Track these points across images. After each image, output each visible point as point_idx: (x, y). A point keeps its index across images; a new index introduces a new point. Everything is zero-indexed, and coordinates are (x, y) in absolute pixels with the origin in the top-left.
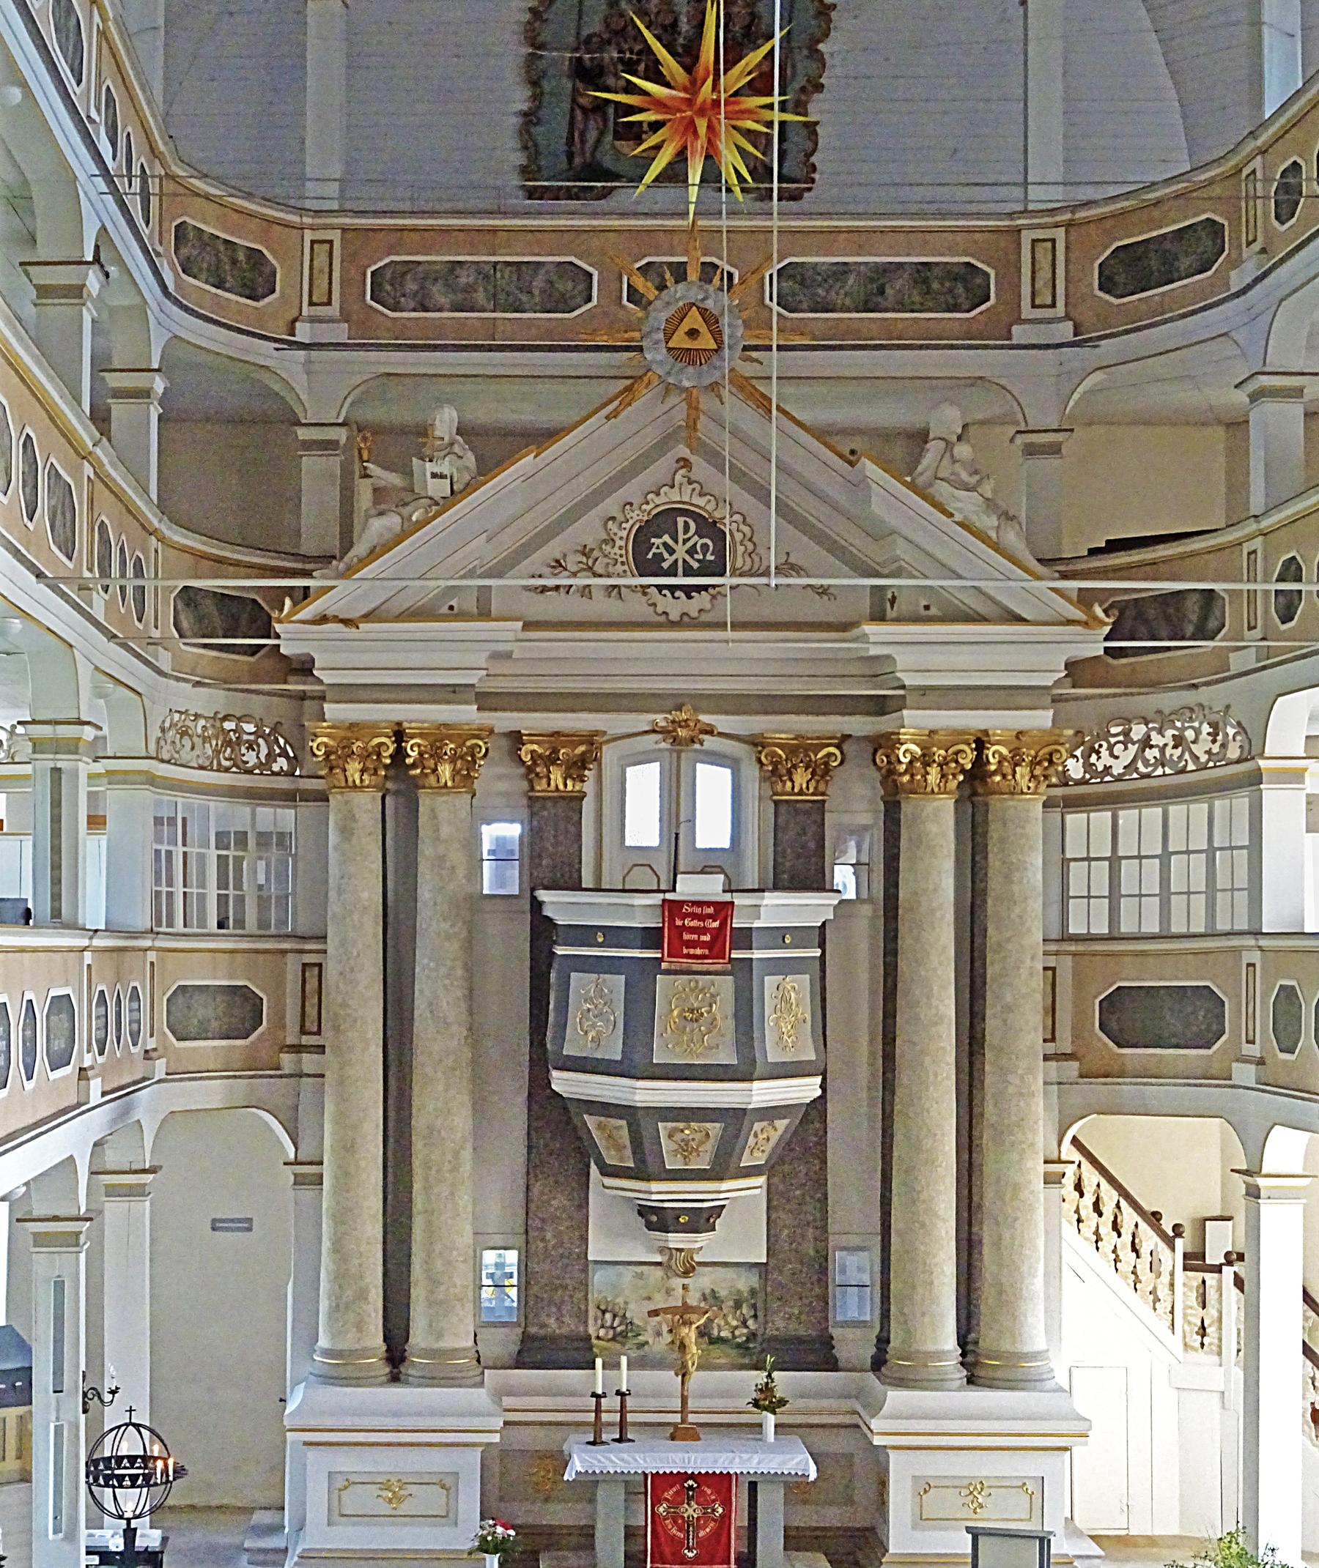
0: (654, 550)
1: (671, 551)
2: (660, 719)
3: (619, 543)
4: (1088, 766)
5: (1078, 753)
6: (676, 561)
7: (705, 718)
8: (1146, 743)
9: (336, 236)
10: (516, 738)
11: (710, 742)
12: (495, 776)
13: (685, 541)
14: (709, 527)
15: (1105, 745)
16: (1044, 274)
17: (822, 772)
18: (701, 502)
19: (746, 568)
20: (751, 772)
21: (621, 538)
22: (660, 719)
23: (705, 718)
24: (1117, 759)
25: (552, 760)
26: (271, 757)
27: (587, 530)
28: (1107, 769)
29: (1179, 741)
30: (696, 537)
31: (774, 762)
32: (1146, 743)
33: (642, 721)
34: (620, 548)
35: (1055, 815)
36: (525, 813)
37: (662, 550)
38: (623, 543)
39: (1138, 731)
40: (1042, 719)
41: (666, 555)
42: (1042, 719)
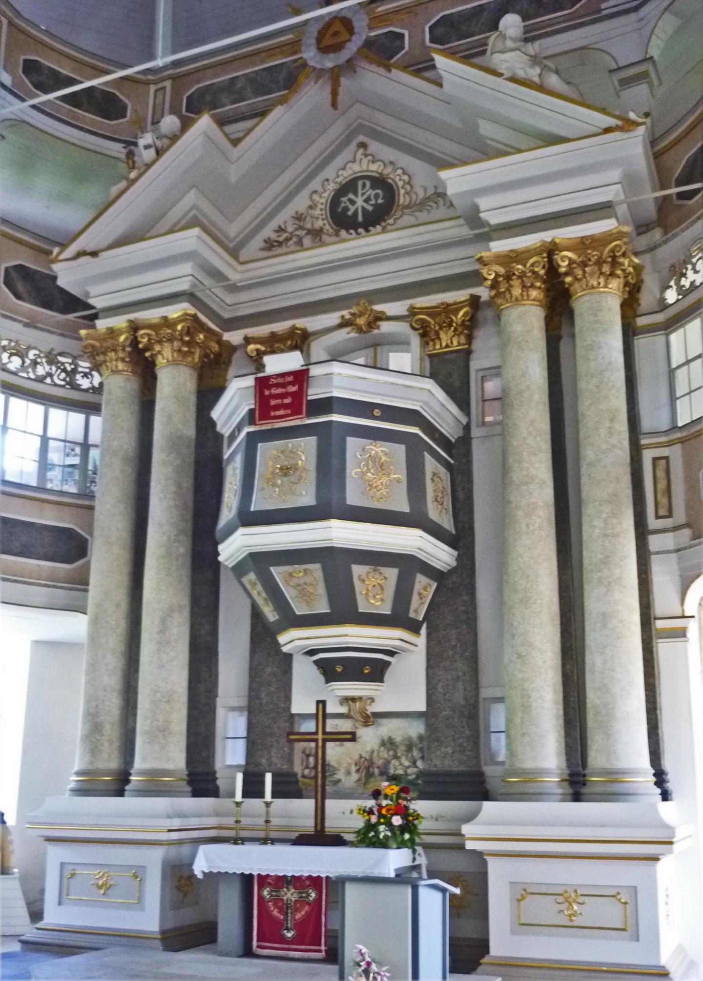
0: (343, 205)
1: (353, 202)
2: (346, 313)
3: (320, 206)
4: (680, 289)
5: (672, 283)
6: (357, 209)
7: (378, 308)
11: (386, 327)
13: (363, 194)
14: (379, 182)
15: (690, 267)
18: (374, 167)
19: (407, 203)
21: (322, 204)
23: (378, 308)
27: (300, 203)
28: (692, 283)
30: (370, 191)
33: (332, 318)
34: (321, 210)
37: (348, 204)
38: (323, 207)
41: (350, 206)
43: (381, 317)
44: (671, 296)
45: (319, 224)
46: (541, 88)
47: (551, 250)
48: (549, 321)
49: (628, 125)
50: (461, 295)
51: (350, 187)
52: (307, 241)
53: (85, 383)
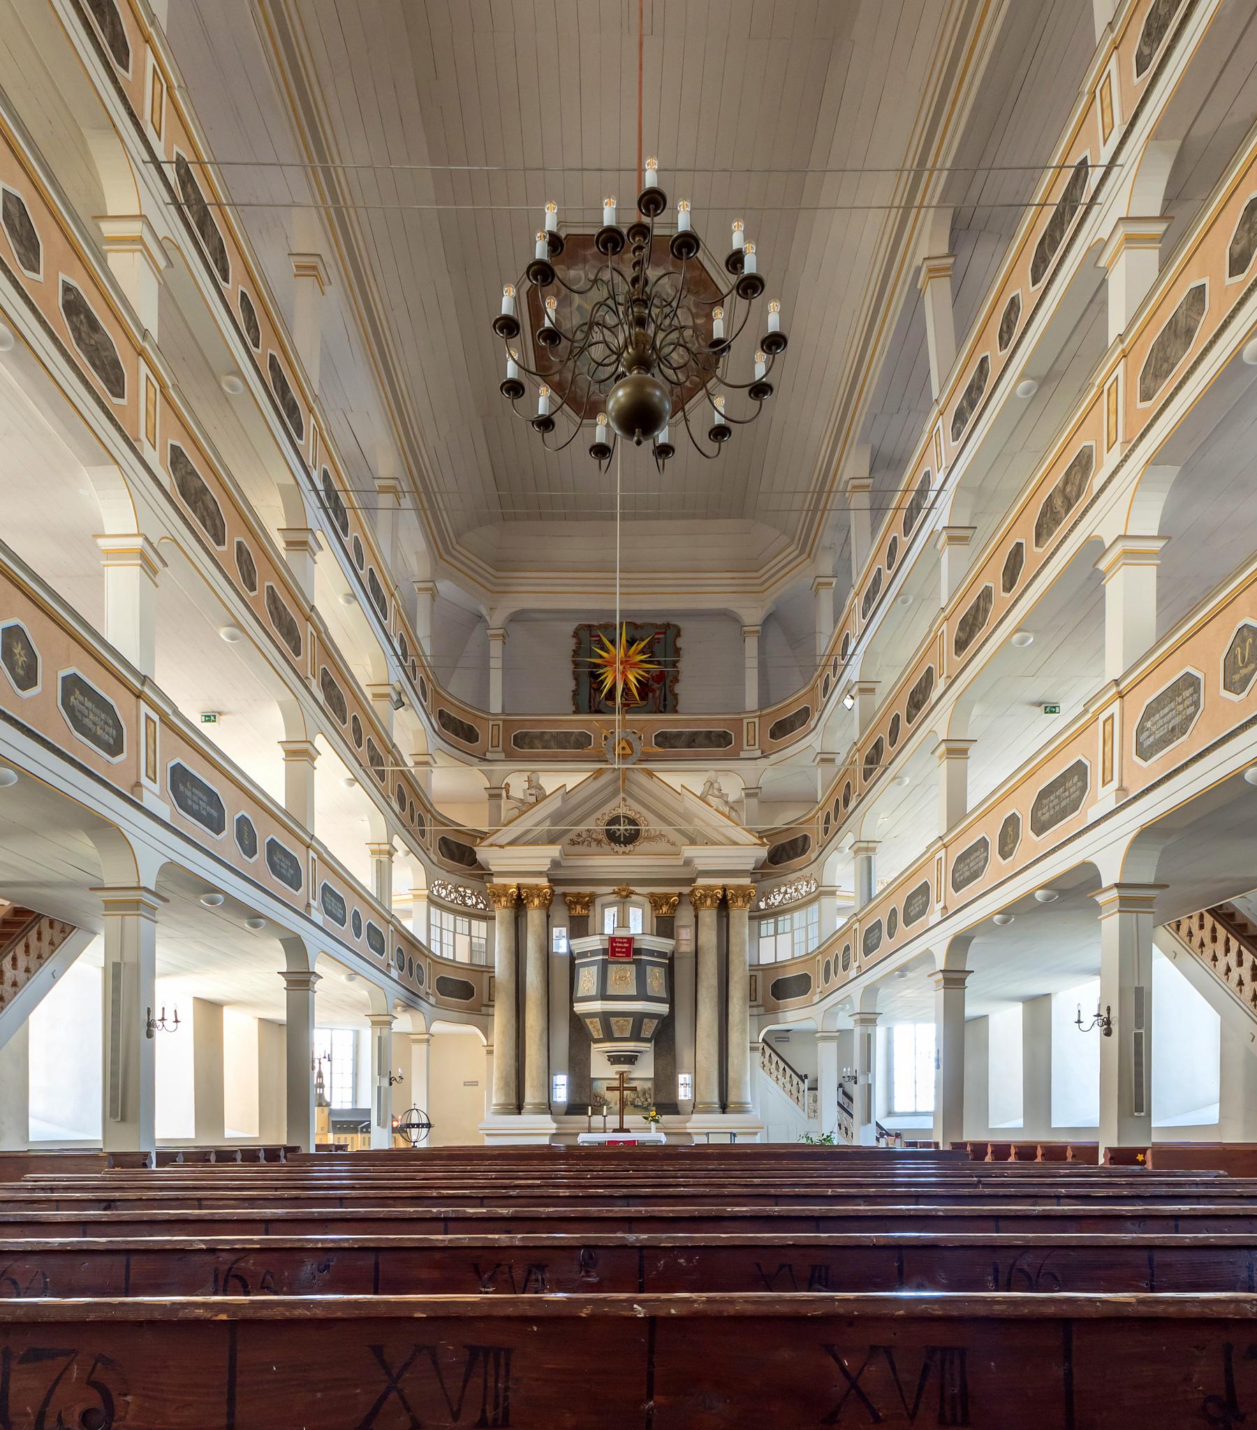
2: (616, 888)
4: (767, 904)
8: (786, 893)
9: (501, 723)
10: (565, 895)
11: (634, 897)
12: (560, 913)
14: (632, 822)
16: (751, 734)
17: (674, 907)
20: (648, 907)
22: (616, 888)
24: (776, 899)
25: (576, 903)
26: (477, 903)
29: (796, 890)
31: (656, 902)
32: (786, 893)
33: (609, 889)
35: (755, 923)
36: (568, 923)
39: (783, 889)
40: (746, 881)
42: (746, 881)
43: (632, 893)
44: (762, 905)
45: (600, 837)
46: (728, 818)
47: (724, 889)
48: (719, 917)
49: (763, 845)
50: (676, 890)
51: (615, 820)
52: (594, 844)
53: (469, 902)
